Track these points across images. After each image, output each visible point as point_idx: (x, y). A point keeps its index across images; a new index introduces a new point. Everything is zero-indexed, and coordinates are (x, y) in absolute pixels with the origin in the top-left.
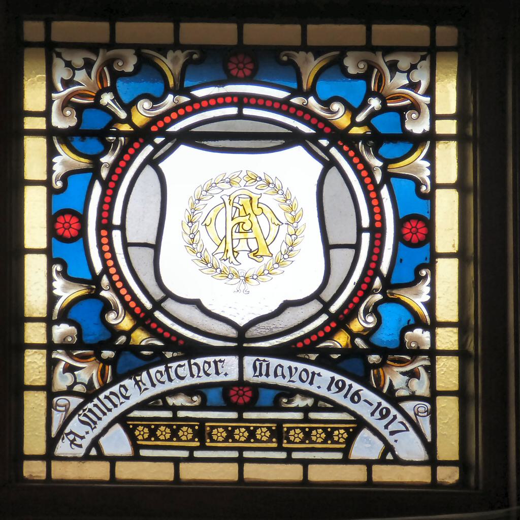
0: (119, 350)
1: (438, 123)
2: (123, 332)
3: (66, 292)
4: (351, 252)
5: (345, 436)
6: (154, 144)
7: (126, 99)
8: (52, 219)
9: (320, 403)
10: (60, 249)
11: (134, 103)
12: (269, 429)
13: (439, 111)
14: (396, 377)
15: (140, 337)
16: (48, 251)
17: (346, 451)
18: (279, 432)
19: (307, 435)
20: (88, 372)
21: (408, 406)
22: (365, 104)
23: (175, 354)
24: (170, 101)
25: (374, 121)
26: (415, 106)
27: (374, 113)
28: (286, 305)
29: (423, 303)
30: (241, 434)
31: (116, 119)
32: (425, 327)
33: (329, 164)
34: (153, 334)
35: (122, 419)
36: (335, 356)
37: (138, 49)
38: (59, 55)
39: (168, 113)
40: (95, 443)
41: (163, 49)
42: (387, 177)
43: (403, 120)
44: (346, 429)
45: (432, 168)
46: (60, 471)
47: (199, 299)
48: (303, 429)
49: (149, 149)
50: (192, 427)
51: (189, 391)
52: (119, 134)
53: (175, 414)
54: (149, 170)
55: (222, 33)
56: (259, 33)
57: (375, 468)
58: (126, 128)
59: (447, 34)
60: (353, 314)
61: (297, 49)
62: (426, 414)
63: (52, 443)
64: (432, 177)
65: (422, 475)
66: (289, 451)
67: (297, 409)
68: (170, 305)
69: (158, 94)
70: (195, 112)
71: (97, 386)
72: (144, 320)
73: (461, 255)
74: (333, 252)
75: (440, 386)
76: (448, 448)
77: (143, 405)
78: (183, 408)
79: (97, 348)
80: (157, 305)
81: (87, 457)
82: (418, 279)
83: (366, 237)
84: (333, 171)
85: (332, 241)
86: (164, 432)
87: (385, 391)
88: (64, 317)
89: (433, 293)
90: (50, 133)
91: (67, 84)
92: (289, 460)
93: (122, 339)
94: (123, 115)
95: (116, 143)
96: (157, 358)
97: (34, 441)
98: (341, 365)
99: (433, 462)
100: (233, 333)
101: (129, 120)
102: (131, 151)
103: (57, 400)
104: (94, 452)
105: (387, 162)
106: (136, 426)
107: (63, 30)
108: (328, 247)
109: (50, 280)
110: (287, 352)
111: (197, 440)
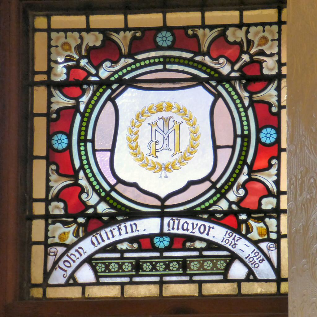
0: (89, 217)
2: (91, 206)
3: (58, 184)
4: (230, 150)
5: (225, 265)
6: (112, 89)
9: (212, 245)
12: (178, 262)
15: (103, 208)
18: (184, 265)
20: (69, 233)
21: (263, 245)
23: (125, 218)
27: (246, 64)
30: (161, 266)
31: (90, 74)
33: (218, 96)
35: (90, 260)
36: (218, 216)
40: (72, 276)
44: (225, 261)
46: (52, 293)
49: (109, 91)
50: (131, 263)
51: (131, 240)
53: (122, 255)
54: (109, 104)
57: (244, 285)
63: (47, 275)
64: (279, 101)
66: (191, 275)
74: (219, 151)
77: (104, 250)
78: (127, 251)
82: (270, 166)
84: (220, 100)
86: (114, 267)
88: (57, 198)
90: (50, 85)
92: (191, 281)
93: (91, 211)
94: (93, 71)
96: (112, 220)
97: (37, 276)
100: (158, 203)
101: (97, 75)
102: (98, 94)
103: (50, 249)
104: (72, 281)
105: (251, 94)
106: (97, 264)
109: (48, 175)
110: (191, 214)
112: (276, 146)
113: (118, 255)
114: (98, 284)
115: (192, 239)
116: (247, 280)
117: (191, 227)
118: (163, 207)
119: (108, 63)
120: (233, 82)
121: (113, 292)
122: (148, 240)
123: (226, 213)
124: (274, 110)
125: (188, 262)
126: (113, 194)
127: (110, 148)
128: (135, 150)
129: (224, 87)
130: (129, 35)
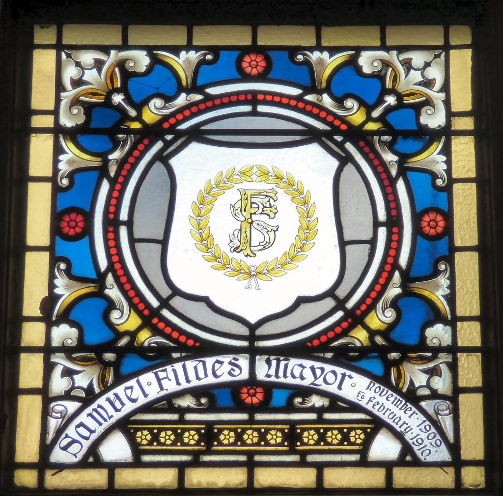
4: (368, 246)
5: (362, 436)
6: (164, 141)
7: (137, 99)
8: (57, 217)
9: (336, 403)
10: (64, 248)
11: (146, 102)
14: (415, 375)
15: (144, 337)
16: (51, 249)
19: (322, 438)
22: (380, 101)
23: (183, 354)
24: (182, 100)
27: (390, 109)
28: (301, 301)
29: (444, 296)
30: (251, 437)
31: (126, 117)
32: (445, 322)
33: (345, 160)
35: (125, 425)
37: (150, 50)
39: (181, 110)
40: (93, 450)
41: (175, 50)
42: (403, 171)
44: (364, 430)
45: (449, 162)
48: (317, 430)
49: (159, 145)
51: (196, 392)
52: (129, 131)
54: (158, 166)
56: (272, 36)
58: (136, 125)
61: (311, 49)
62: (447, 412)
64: (449, 171)
65: (444, 479)
66: (304, 454)
67: (312, 409)
68: (177, 302)
70: (208, 110)
71: (97, 390)
72: (150, 318)
76: (474, 446)
77: (148, 408)
80: (165, 303)
81: (83, 464)
82: (436, 273)
83: (382, 232)
85: (347, 237)
86: (167, 437)
89: (452, 286)
91: (77, 83)
92: (303, 464)
94: (133, 113)
95: (125, 142)
97: (27, 447)
99: (457, 463)
100: (245, 331)
101: (139, 118)
104: (92, 459)
105: (403, 158)
108: (343, 244)
109: (52, 277)
111: (202, 444)
113: (175, 417)
114: (137, 463)
115: (307, 392)
116: (401, 462)
117: (300, 371)
119: (157, 102)
121: (165, 478)
122: (227, 392)
123: (364, 352)
124: (439, 182)
126: (166, 313)
127: (160, 237)
128: (205, 241)
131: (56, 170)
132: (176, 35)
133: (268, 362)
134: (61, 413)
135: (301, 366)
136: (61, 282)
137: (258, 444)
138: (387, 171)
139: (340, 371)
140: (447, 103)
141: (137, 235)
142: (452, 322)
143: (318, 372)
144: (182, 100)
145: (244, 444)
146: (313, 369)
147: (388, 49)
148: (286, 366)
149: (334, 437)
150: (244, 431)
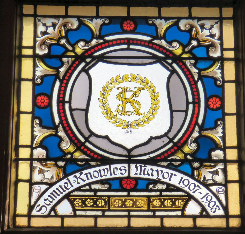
0: (67, 161)
1: (225, 52)
3: (41, 134)
4: (184, 114)
6: (86, 62)
8: (35, 97)
9: (170, 187)
10: (38, 112)
13: (225, 46)
15: (78, 155)
16: (32, 113)
17: (183, 210)
20: (51, 173)
25: (194, 51)
26: (213, 45)
27: (194, 47)
28: (152, 138)
29: (220, 137)
31: (67, 50)
32: (221, 149)
33: (173, 72)
34: (85, 153)
35: (67, 197)
37: (78, 18)
38: (39, 20)
40: (53, 209)
41: (91, 18)
42: (201, 77)
43: (208, 51)
44: (183, 200)
45: (223, 73)
46: (36, 223)
47: (108, 135)
50: (104, 200)
51: (102, 182)
54: (83, 74)
55: (120, 11)
56: (137, 12)
59: (228, 12)
60: (185, 143)
61: (156, 18)
62: (223, 192)
64: (223, 77)
65: (221, 223)
66: (154, 211)
68: (92, 139)
69: (88, 40)
72: (79, 146)
73: (238, 114)
75: (229, 178)
76: (235, 208)
77: (78, 189)
79: (56, 160)
80: (87, 139)
82: (216, 126)
83: (191, 107)
85: (174, 109)
86: (89, 202)
87: (202, 180)
89: (224, 133)
92: (154, 216)
93: (69, 156)
94: (70, 48)
98: (180, 168)
99: (227, 216)
100: (125, 153)
101: (73, 51)
104: (53, 212)
105: (200, 70)
106: (75, 200)
107: (42, 10)
109: (33, 127)
110: (153, 162)
112: (220, 111)
114: (75, 216)
115: (156, 182)
116: (201, 216)
118: (129, 156)
120: (185, 61)
125: (151, 200)
126: (88, 144)
129: (178, 65)
130: (99, 22)
131: (34, 75)
132: (91, 11)
133: (136, 167)
134: (39, 190)
135: (152, 169)
136: (37, 129)
137: (133, 206)
138: (193, 77)
139: (170, 171)
140: (222, 44)
141: (73, 107)
142: (224, 149)
143: (160, 173)
144: (94, 42)
145: (126, 206)
146: (157, 171)
147: (193, 18)
148: (145, 170)
149: (168, 203)
150: (126, 200)
